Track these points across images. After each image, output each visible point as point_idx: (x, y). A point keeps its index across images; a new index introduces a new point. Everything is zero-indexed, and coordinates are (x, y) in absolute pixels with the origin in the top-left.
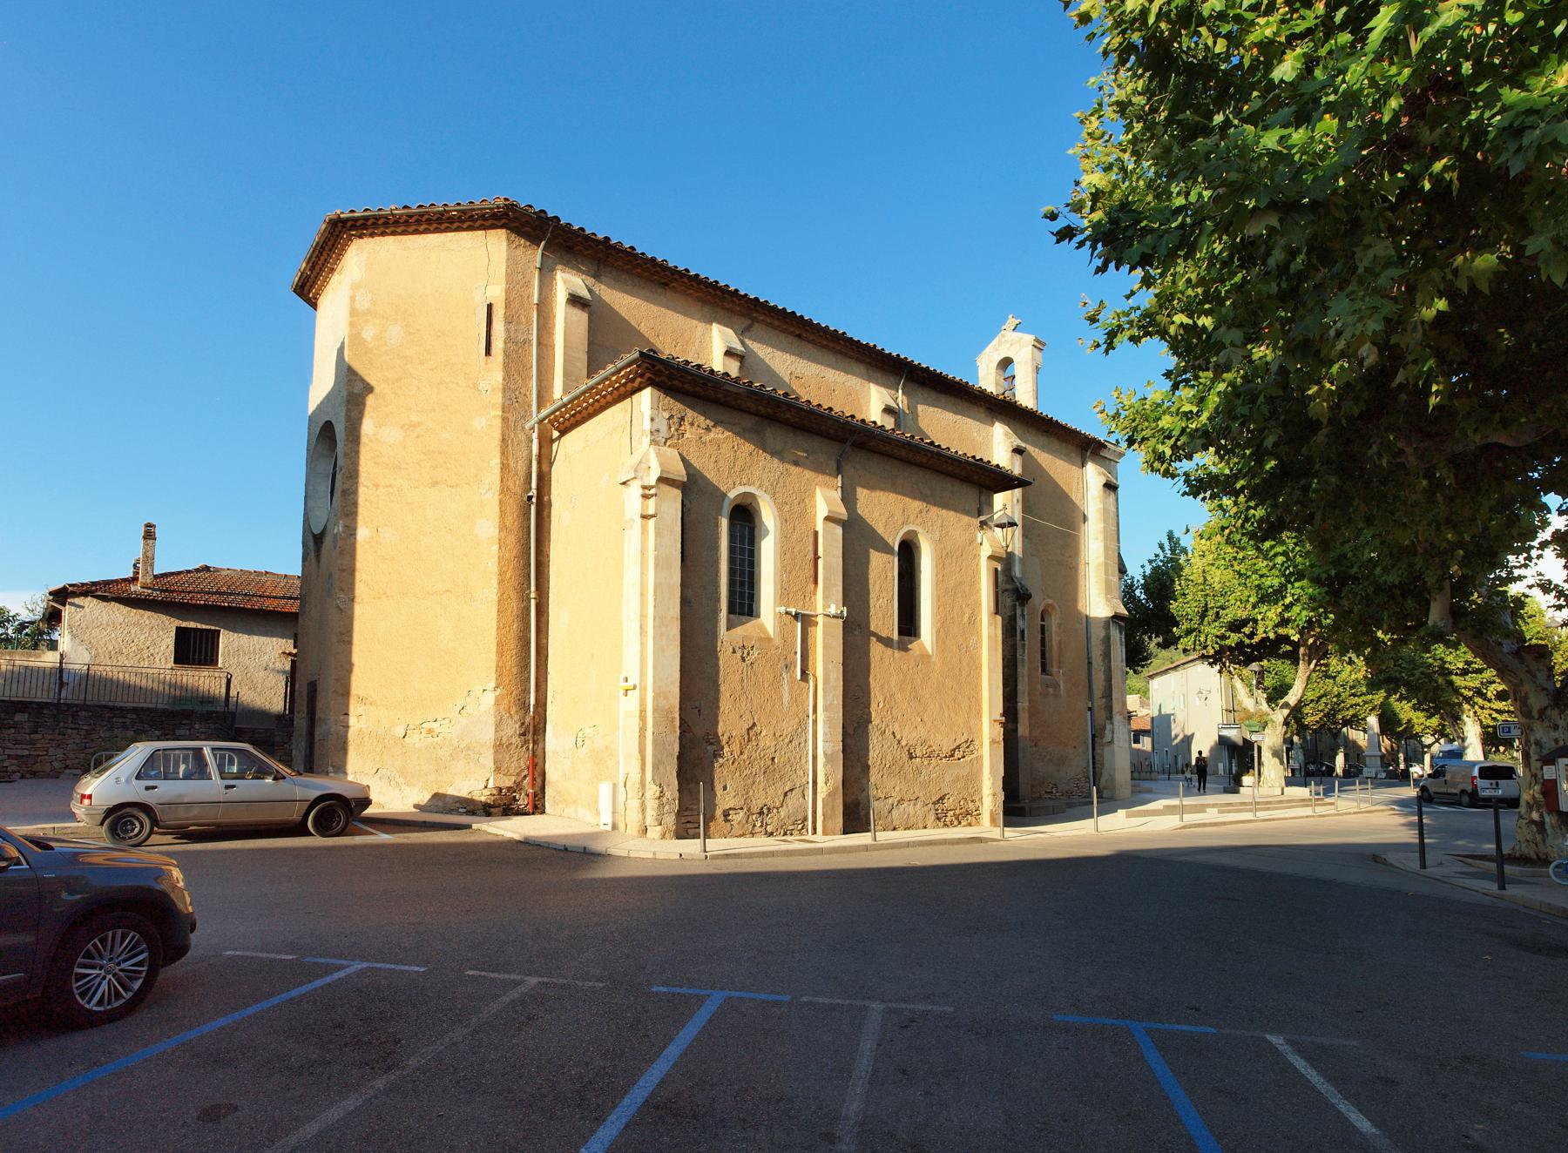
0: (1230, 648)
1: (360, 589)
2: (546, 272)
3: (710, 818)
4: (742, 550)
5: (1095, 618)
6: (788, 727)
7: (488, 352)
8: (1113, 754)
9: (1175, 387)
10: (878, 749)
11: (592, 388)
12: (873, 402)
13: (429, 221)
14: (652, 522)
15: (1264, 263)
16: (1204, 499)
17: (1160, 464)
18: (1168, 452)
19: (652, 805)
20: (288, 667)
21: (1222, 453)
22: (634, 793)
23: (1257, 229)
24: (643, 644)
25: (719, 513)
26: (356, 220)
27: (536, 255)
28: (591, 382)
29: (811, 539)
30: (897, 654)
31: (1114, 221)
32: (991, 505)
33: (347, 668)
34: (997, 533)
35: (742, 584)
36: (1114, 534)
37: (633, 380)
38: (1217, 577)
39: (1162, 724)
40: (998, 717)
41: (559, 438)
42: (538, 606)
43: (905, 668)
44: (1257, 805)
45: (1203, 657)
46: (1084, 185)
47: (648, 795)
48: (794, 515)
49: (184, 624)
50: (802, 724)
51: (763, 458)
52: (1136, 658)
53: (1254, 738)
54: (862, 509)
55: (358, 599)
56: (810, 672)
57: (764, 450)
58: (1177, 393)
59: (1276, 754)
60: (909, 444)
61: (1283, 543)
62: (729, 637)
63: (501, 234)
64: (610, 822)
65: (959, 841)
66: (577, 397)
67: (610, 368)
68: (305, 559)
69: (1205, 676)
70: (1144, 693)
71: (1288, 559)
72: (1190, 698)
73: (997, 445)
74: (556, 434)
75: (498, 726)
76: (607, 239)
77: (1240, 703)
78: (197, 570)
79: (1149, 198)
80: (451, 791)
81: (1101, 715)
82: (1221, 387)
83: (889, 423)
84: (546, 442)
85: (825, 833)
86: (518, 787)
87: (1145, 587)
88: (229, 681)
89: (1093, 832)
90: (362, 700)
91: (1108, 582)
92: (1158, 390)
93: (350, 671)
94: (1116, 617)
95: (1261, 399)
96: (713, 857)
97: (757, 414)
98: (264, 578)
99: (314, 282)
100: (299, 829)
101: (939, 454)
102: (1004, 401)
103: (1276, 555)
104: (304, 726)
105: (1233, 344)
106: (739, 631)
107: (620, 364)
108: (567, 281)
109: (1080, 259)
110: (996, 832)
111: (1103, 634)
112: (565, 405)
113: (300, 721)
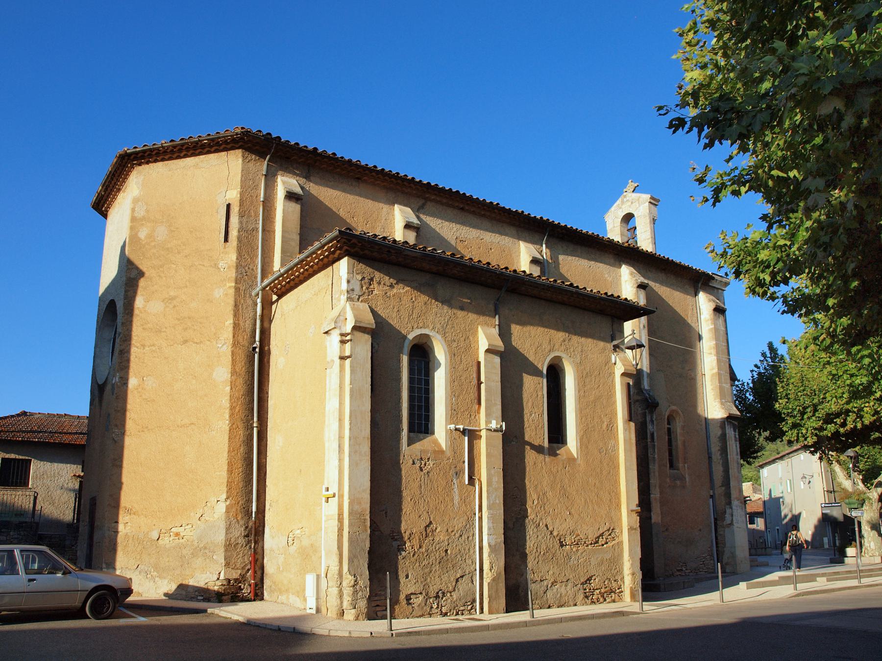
1: (130, 425)
2: (270, 177)
3: (395, 602)
4: (420, 380)
5: (713, 420)
6: (458, 523)
9: (770, 227)
10: (533, 540)
11: (302, 261)
12: (523, 256)
13: (188, 149)
14: (348, 361)
16: (800, 316)
17: (759, 289)
18: (768, 279)
19: (347, 591)
20: (77, 487)
22: (333, 583)
24: (341, 460)
25: (401, 351)
26: (136, 153)
27: (263, 166)
29: (475, 368)
30: (548, 458)
32: (622, 331)
33: (118, 485)
34: (627, 355)
35: (420, 407)
37: (334, 252)
39: (773, 505)
40: (634, 507)
41: (277, 301)
42: (259, 433)
44: (860, 573)
45: (805, 448)
47: (345, 584)
48: (461, 349)
49: (7, 456)
50: (470, 521)
52: (749, 452)
53: (854, 514)
54: (516, 342)
55: (127, 433)
56: (476, 478)
57: (437, 300)
59: (875, 527)
60: (552, 287)
61: (868, 347)
62: (408, 451)
63: (239, 152)
64: (314, 606)
66: (291, 269)
67: (317, 244)
69: (808, 463)
70: (756, 480)
71: (873, 360)
72: (796, 483)
73: (626, 283)
74: (275, 297)
75: (228, 529)
76: (315, 149)
77: (840, 485)
78: (18, 415)
80: (192, 582)
82: (808, 224)
83: (536, 271)
85: (490, 612)
86: (242, 579)
87: (755, 390)
88: (35, 498)
90: (129, 511)
91: (721, 389)
92: (758, 230)
93: (120, 489)
94: (730, 418)
96: (398, 635)
97: (430, 272)
98: (63, 419)
99: (106, 200)
100: (78, 613)
101: (577, 293)
102: (628, 247)
103: (862, 357)
104: (87, 533)
106: (418, 446)
107: (323, 241)
108: (285, 183)
110: (636, 607)
111: (719, 433)
112: (282, 275)
113: (84, 529)
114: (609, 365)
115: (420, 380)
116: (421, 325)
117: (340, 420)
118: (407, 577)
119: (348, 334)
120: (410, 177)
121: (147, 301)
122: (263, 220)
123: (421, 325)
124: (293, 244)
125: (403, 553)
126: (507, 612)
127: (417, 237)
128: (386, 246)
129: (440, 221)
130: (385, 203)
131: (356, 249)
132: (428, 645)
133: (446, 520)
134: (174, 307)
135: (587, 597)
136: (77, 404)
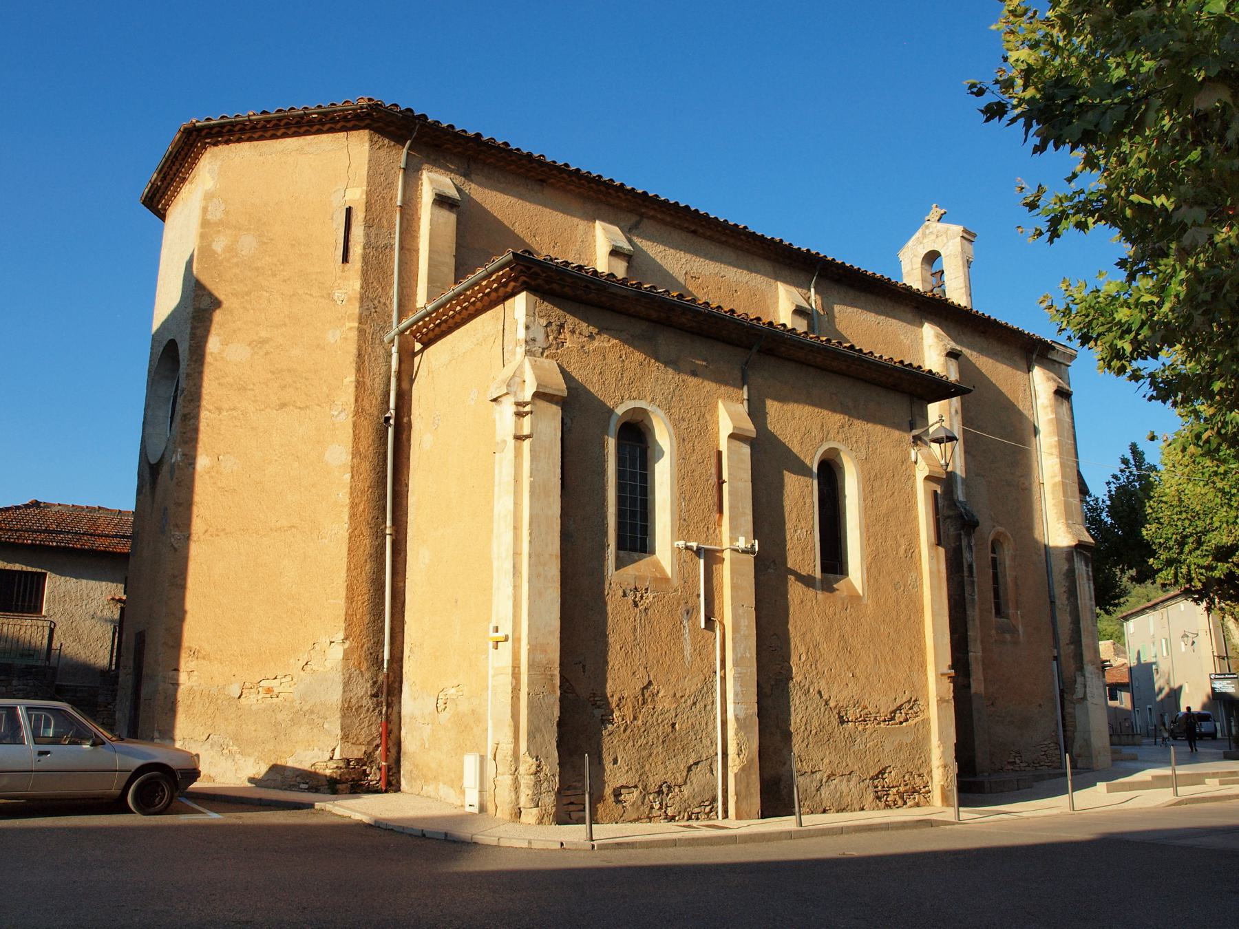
0: (1219, 581)
1: (197, 526)
2: (411, 172)
3: (597, 798)
4: (633, 475)
5: (1056, 548)
6: (691, 685)
7: (345, 259)
8: (1087, 714)
9: (1132, 277)
10: (800, 713)
11: (459, 294)
12: (783, 304)
13: (288, 125)
14: (527, 443)
15: (1221, 139)
19: (526, 781)
20: (117, 616)
21: (1193, 352)
23: (1209, 101)
24: (516, 587)
25: (605, 431)
26: (211, 127)
28: (458, 288)
29: (714, 461)
30: (820, 595)
31: (1049, 98)
34: (934, 450)
35: (633, 514)
36: (1071, 448)
38: (1198, 493)
39: (1142, 674)
40: (946, 670)
41: (422, 351)
43: (830, 612)
45: (1187, 593)
46: (1011, 60)
47: (522, 769)
48: (694, 433)
50: (708, 682)
51: (656, 370)
52: (1108, 596)
55: (194, 537)
56: (716, 619)
57: (657, 360)
58: (1134, 284)
60: (825, 349)
62: (618, 578)
63: (365, 134)
64: (476, 802)
65: (904, 825)
66: (443, 305)
67: (480, 272)
68: (139, 491)
69: (1190, 616)
70: (1118, 638)
73: (930, 349)
74: (418, 346)
75: (347, 684)
76: (478, 135)
78: (27, 506)
79: (1084, 75)
80: (291, 762)
81: (1069, 666)
82: (1183, 275)
83: (801, 326)
84: (407, 356)
85: (739, 817)
86: (368, 759)
87: (1112, 511)
88: (52, 631)
89: (1067, 810)
90: (195, 653)
91: (1067, 505)
92: (1112, 282)
93: (182, 619)
94: (1080, 547)
95: (1227, 286)
96: (603, 847)
98: (97, 515)
99: (164, 193)
100: (116, 805)
101: (859, 358)
102: (933, 298)
104: (131, 686)
105: (1195, 224)
106: (630, 570)
108: (432, 182)
109: (1012, 138)
110: (949, 814)
111: (1065, 567)
112: (429, 314)
113: (126, 679)
114: (907, 466)
115: (633, 475)
116: (634, 394)
117: (515, 528)
118: (615, 761)
119: (527, 404)
120: (617, 183)
121: (225, 343)
122: (401, 233)
123: (634, 394)
124: (446, 270)
125: (610, 727)
126: (763, 816)
127: (629, 268)
128: (582, 279)
129: (662, 248)
130: (581, 218)
131: (539, 281)
132: (645, 862)
133: (673, 680)
134: (267, 353)
135: (879, 798)
136: (119, 494)
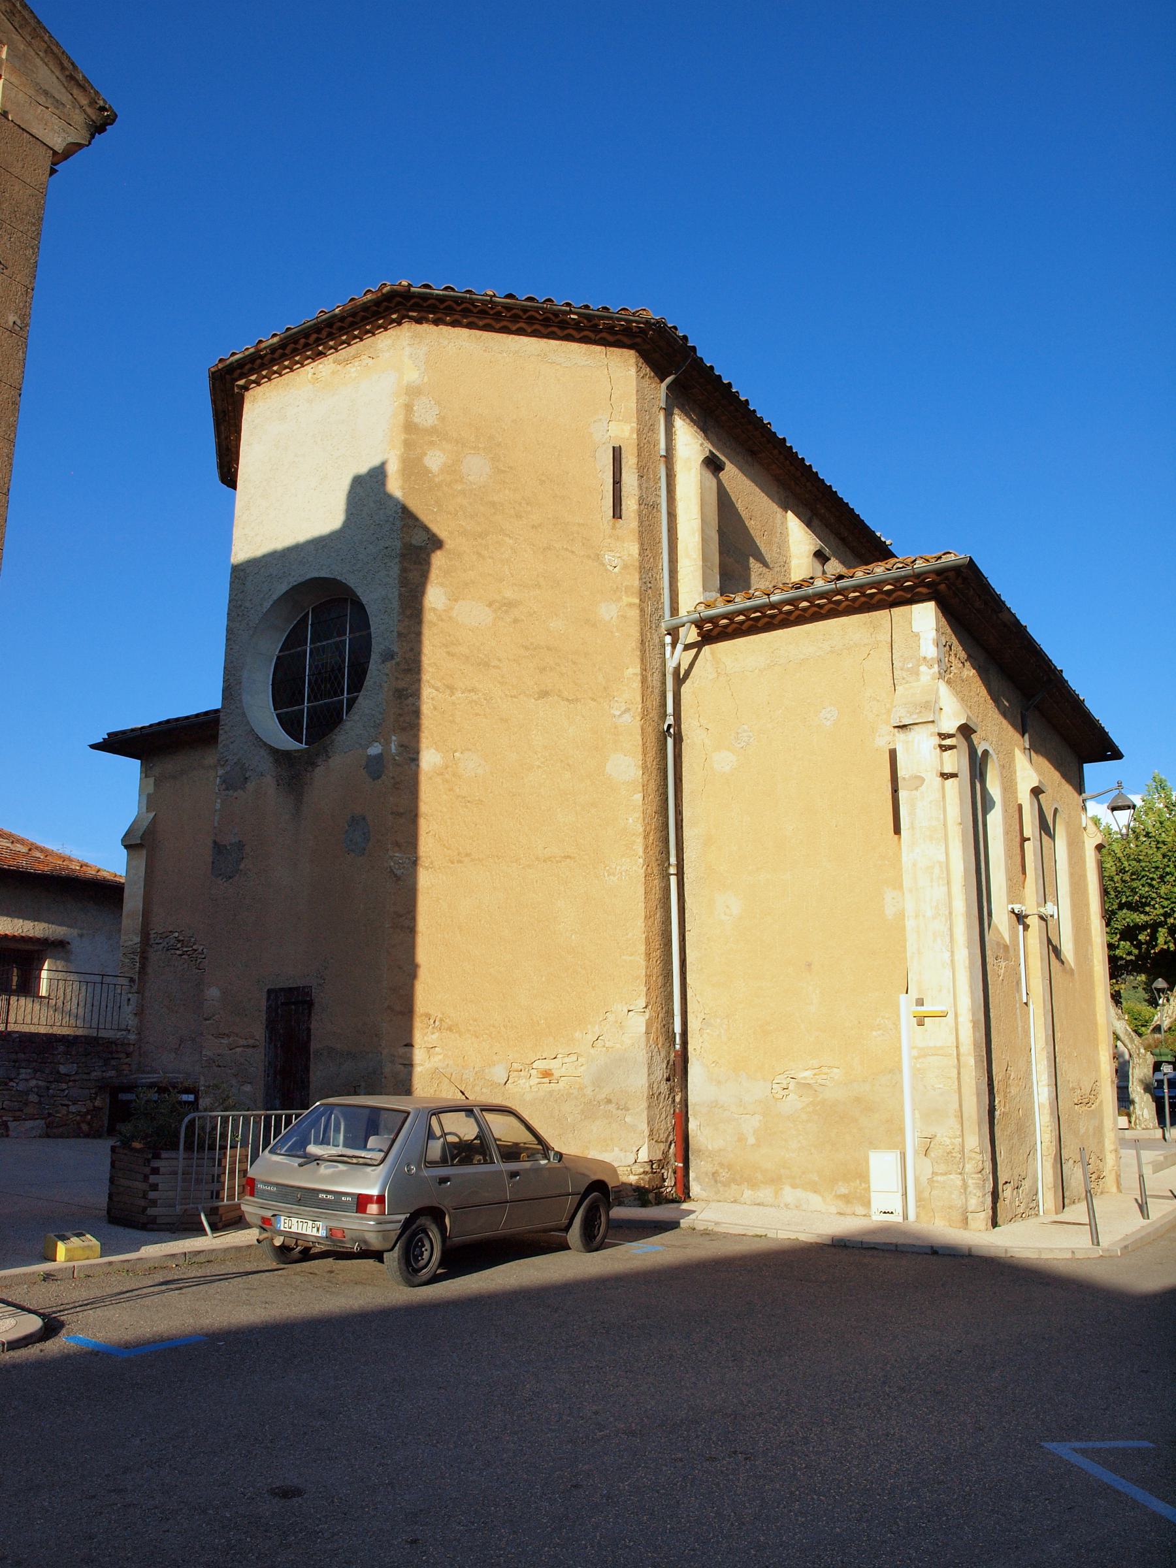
1: (427, 845)
7: (617, 513)
134: (516, 621)
